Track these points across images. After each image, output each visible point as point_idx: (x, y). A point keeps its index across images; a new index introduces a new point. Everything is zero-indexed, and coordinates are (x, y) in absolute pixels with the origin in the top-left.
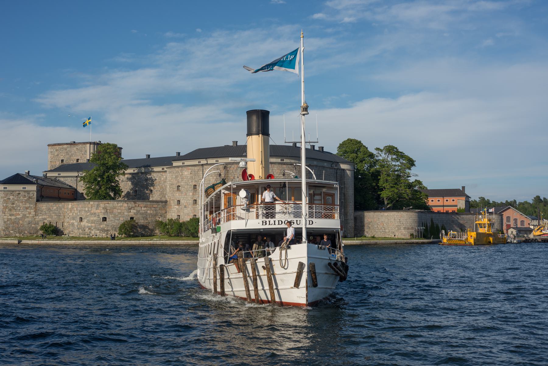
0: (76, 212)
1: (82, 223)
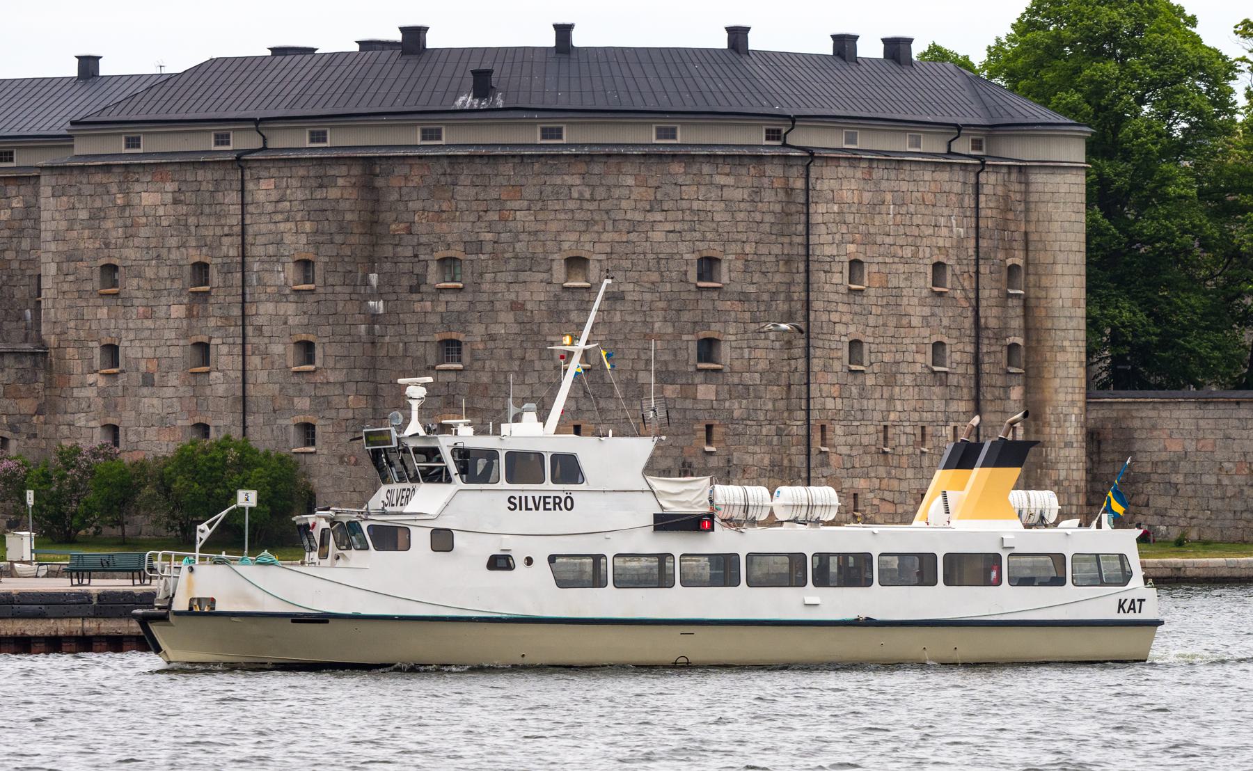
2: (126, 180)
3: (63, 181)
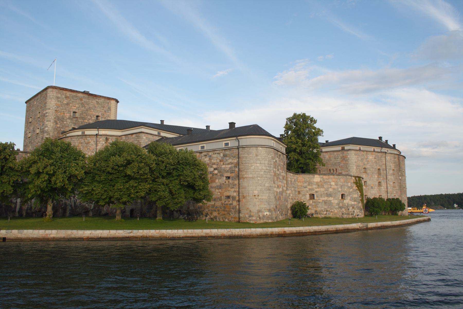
0: (336, 187)
1: (345, 201)
2: (367, 154)
3: (357, 153)
